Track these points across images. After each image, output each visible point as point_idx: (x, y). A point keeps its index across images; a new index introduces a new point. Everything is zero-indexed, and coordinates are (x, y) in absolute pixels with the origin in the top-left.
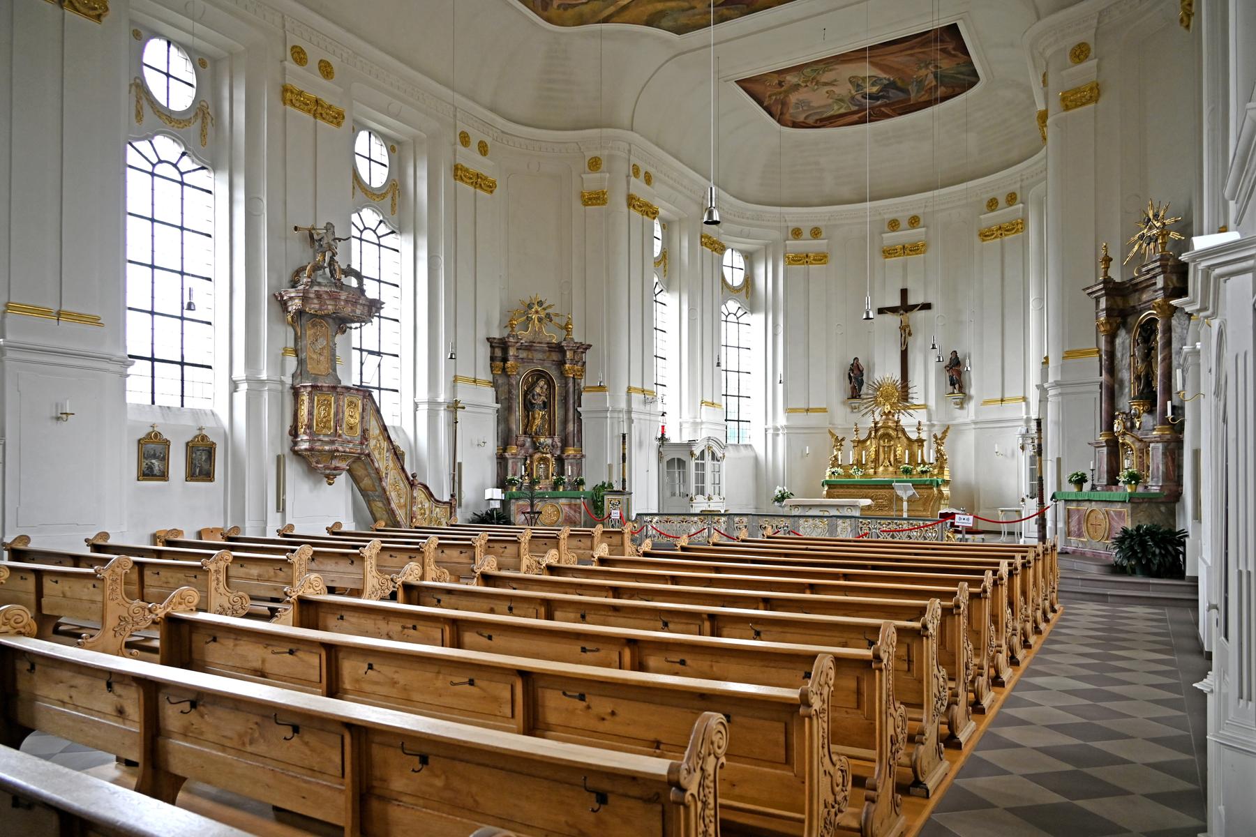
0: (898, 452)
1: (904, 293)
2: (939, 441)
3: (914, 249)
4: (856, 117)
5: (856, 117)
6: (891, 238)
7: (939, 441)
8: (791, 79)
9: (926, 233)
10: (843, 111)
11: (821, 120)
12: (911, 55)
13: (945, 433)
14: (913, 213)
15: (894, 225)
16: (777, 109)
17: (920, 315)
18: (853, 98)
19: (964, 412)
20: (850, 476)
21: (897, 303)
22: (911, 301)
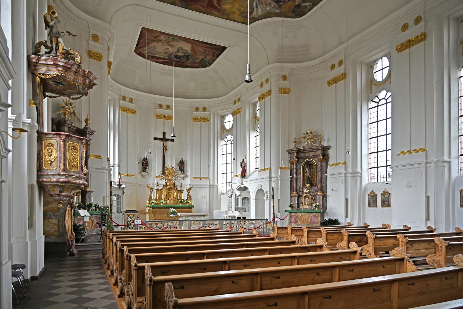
0: (175, 195)
1: (164, 133)
2: (188, 191)
3: (169, 118)
4: (162, 61)
5: (162, 61)
6: (160, 111)
7: (188, 191)
8: (162, 37)
9: (209, 114)
10: (162, 57)
11: (149, 56)
12: (205, 50)
13: (191, 188)
14: (168, 104)
15: (160, 106)
16: (140, 45)
17: (169, 143)
18: (171, 54)
19: (184, 181)
20: (159, 204)
21: (161, 137)
22: (167, 137)
